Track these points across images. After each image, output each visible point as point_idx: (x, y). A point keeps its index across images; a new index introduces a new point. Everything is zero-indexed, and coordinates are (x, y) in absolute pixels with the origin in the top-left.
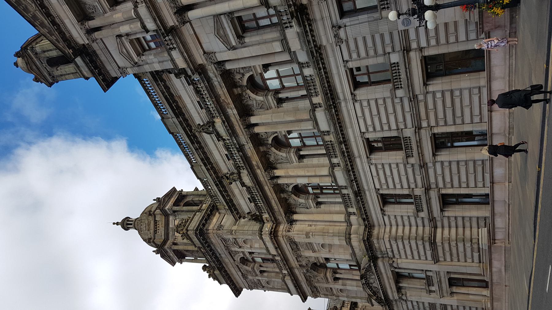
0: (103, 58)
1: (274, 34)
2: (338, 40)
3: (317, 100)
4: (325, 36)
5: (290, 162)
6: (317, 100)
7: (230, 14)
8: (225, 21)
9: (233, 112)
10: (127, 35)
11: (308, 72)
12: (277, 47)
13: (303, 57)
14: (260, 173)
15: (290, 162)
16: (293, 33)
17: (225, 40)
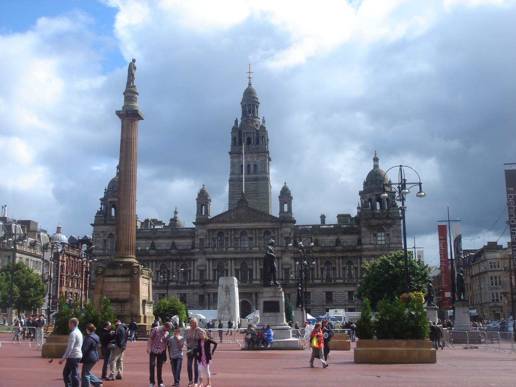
0: (201, 226)
1: (199, 279)
2: (194, 294)
3: (179, 284)
4: (196, 291)
5: (156, 267)
6: (179, 284)
7: (206, 270)
8: (204, 268)
9: (179, 257)
10: (206, 238)
11: (187, 283)
12: (196, 279)
13: (192, 283)
14: (154, 258)
15: (156, 267)
16: (198, 283)
17: (200, 266)
